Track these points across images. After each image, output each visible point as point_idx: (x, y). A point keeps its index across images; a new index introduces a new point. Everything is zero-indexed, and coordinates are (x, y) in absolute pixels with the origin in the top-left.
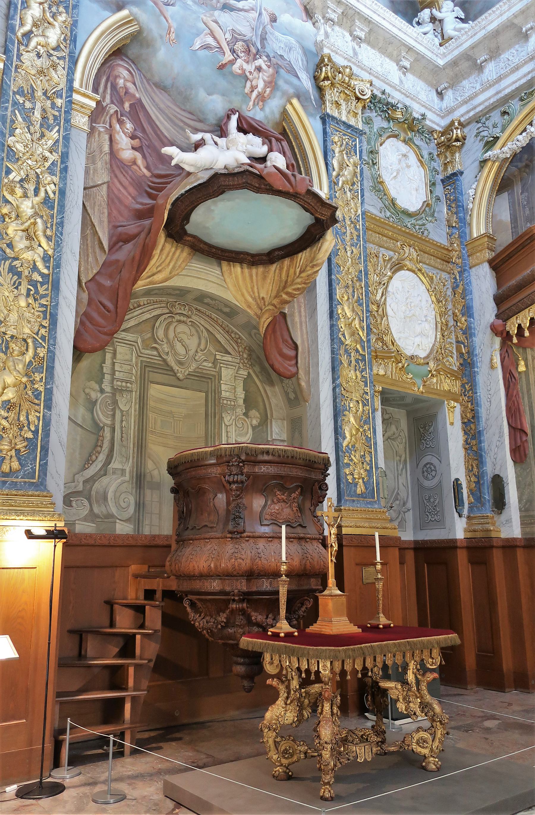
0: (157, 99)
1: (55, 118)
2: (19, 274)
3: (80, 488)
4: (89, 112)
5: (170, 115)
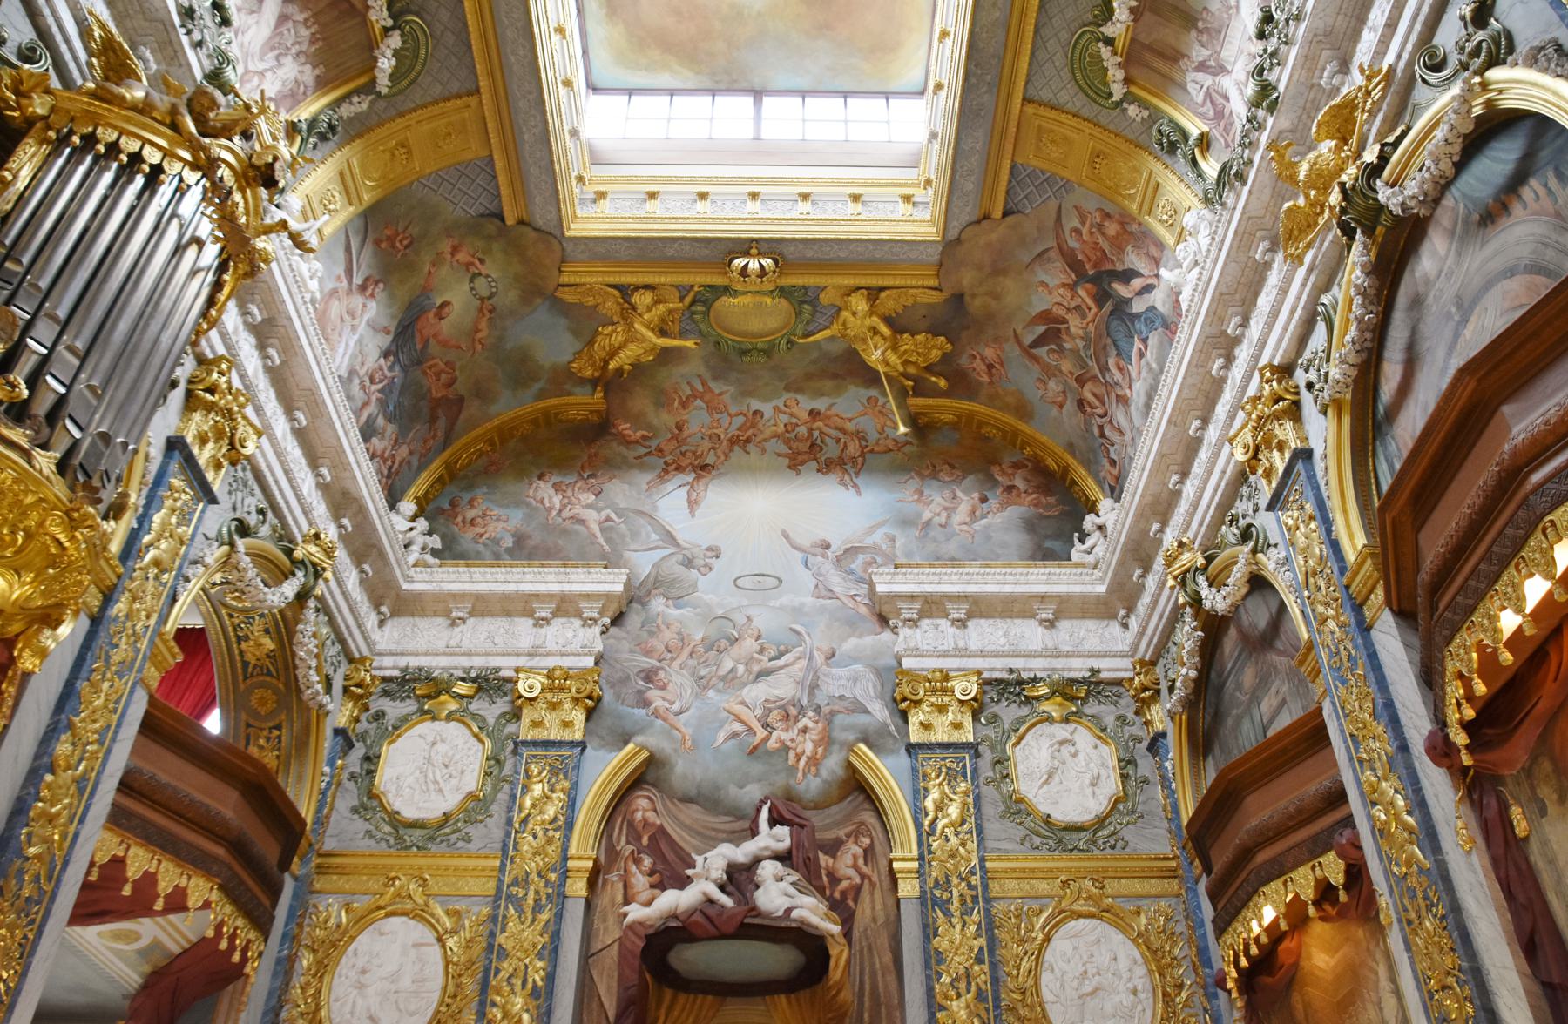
0: (682, 817)
1: (548, 895)
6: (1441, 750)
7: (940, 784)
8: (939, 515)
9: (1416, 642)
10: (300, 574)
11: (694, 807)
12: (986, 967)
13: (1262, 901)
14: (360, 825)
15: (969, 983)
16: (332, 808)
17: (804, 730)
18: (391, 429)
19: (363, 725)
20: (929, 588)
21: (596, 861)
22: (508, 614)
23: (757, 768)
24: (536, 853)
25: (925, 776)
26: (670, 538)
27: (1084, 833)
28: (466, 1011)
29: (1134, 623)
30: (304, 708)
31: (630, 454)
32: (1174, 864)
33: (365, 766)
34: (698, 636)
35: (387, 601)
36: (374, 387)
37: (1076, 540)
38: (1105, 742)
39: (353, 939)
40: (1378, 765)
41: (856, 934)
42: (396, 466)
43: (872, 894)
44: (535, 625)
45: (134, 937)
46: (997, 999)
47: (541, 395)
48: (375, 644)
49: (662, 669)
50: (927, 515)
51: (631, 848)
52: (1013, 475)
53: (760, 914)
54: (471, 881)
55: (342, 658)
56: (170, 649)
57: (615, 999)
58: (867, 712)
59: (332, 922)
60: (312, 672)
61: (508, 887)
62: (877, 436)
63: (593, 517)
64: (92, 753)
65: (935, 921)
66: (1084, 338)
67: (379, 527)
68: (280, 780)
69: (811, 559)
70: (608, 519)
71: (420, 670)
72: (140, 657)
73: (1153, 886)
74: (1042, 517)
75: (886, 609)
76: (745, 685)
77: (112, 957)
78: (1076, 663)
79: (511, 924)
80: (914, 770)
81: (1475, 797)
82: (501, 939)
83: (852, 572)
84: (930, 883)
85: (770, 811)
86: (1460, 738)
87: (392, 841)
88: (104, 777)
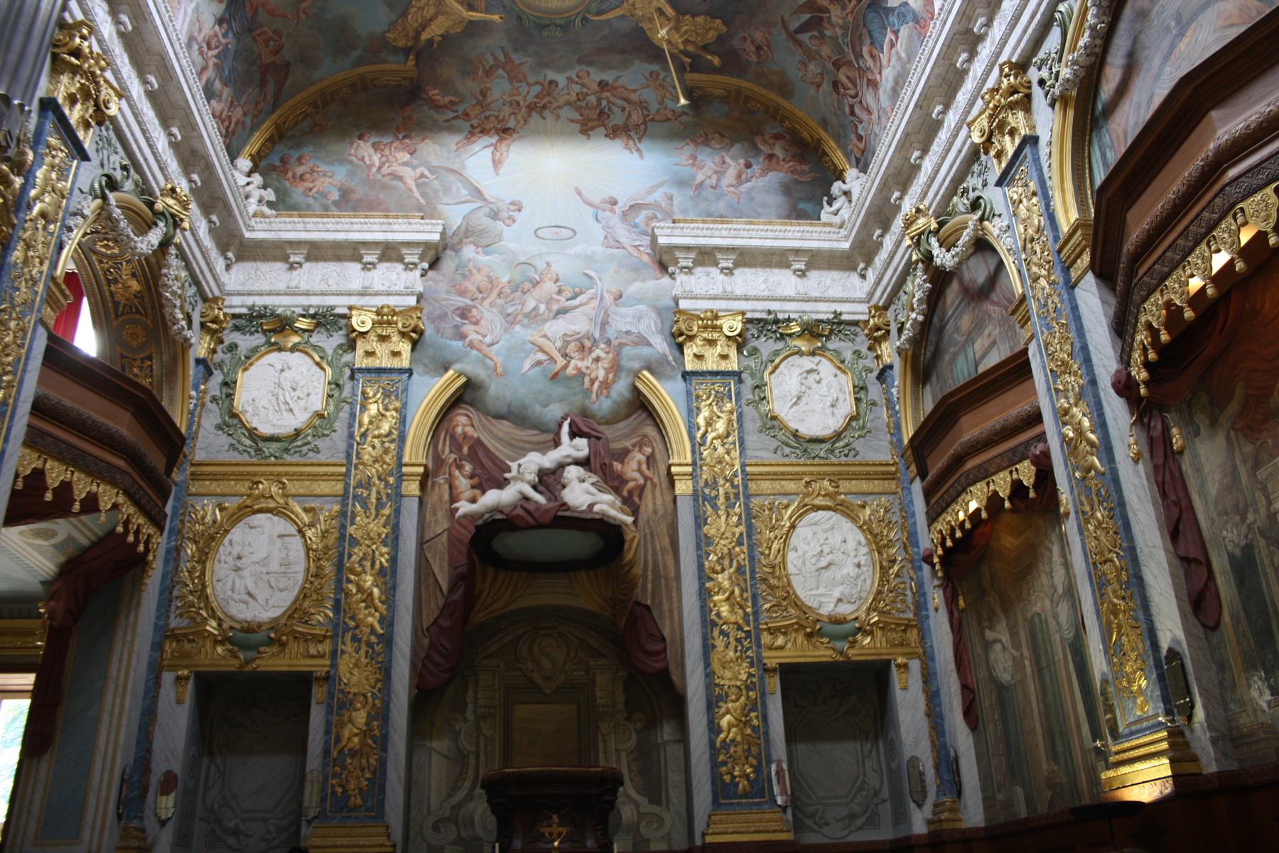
0: (495, 431)
1: (388, 495)
2: (359, 640)
3: (448, 814)
4: (419, 478)
5: (513, 442)
6: (1125, 387)
7: (710, 404)
8: (710, 177)
9: (1113, 301)
10: (161, 224)
11: (506, 423)
12: (745, 548)
13: (969, 497)
14: (224, 440)
15: (731, 561)
16: (199, 426)
17: (597, 360)
18: (227, 92)
19: (219, 356)
20: (702, 241)
21: (426, 466)
22: (339, 259)
23: (558, 390)
24: (376, 461)
25: (698, 397)
26: (478, 193)
27: (823, 445)
28: (326, 586)
29: (871, 275)
30: (171, 341)
31: (441, 117)
32: (893, 469)
33: (224, 390)
34: (505, 279)
35: (233, 248)
36: (211, 53)
37: (825, 204)
38: (844, 372)
39: (227, 531)
40: (1071, 394)
41: (641, 523)
42: (232, 126)
43: (653, 492)
44: (363, 269)
45: (52, 534)
46: (753, 572)
47: (359, 62)
48: (224, 285)
49: (475, 307)
50: (700, 177)
51: (453, 456)
52: (774, 144)
53: (569, 509)
54: (323, 484)
55: (198, 298)
56: (62, 291)
57: (446, 576)
58: (649, 344)
59: (209, 519)
60: (177, 311)
61: (354, 488)
62: (658, 106)
63: (409, 174)
64: (9, 382)
65: (705, 513)
66: (844, 27)
67: (224, 182)
68: (165, 404)
69: (600, 214)
70: (422, 176)
71: (265, 308)
72: (38, 299)
73: (877, 485)
74: (797, 182)
75: (666, 258)
76: (546, 321)
77: (29, 549)
78: (822, 307)
79: (358, 518)
80: (689, 393)
81: (1146, 420)
82: (351, 530)
83: (636, 226)
84: (702, 483)
85: (570, 425)
86: (1141, 375)
87: (253, 453)
88: (20, 404)
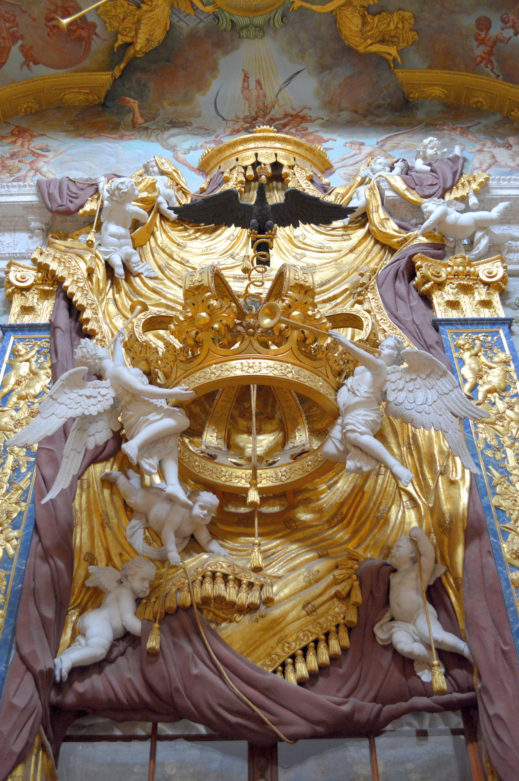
7: (476, 355)
25: (459, 347)
